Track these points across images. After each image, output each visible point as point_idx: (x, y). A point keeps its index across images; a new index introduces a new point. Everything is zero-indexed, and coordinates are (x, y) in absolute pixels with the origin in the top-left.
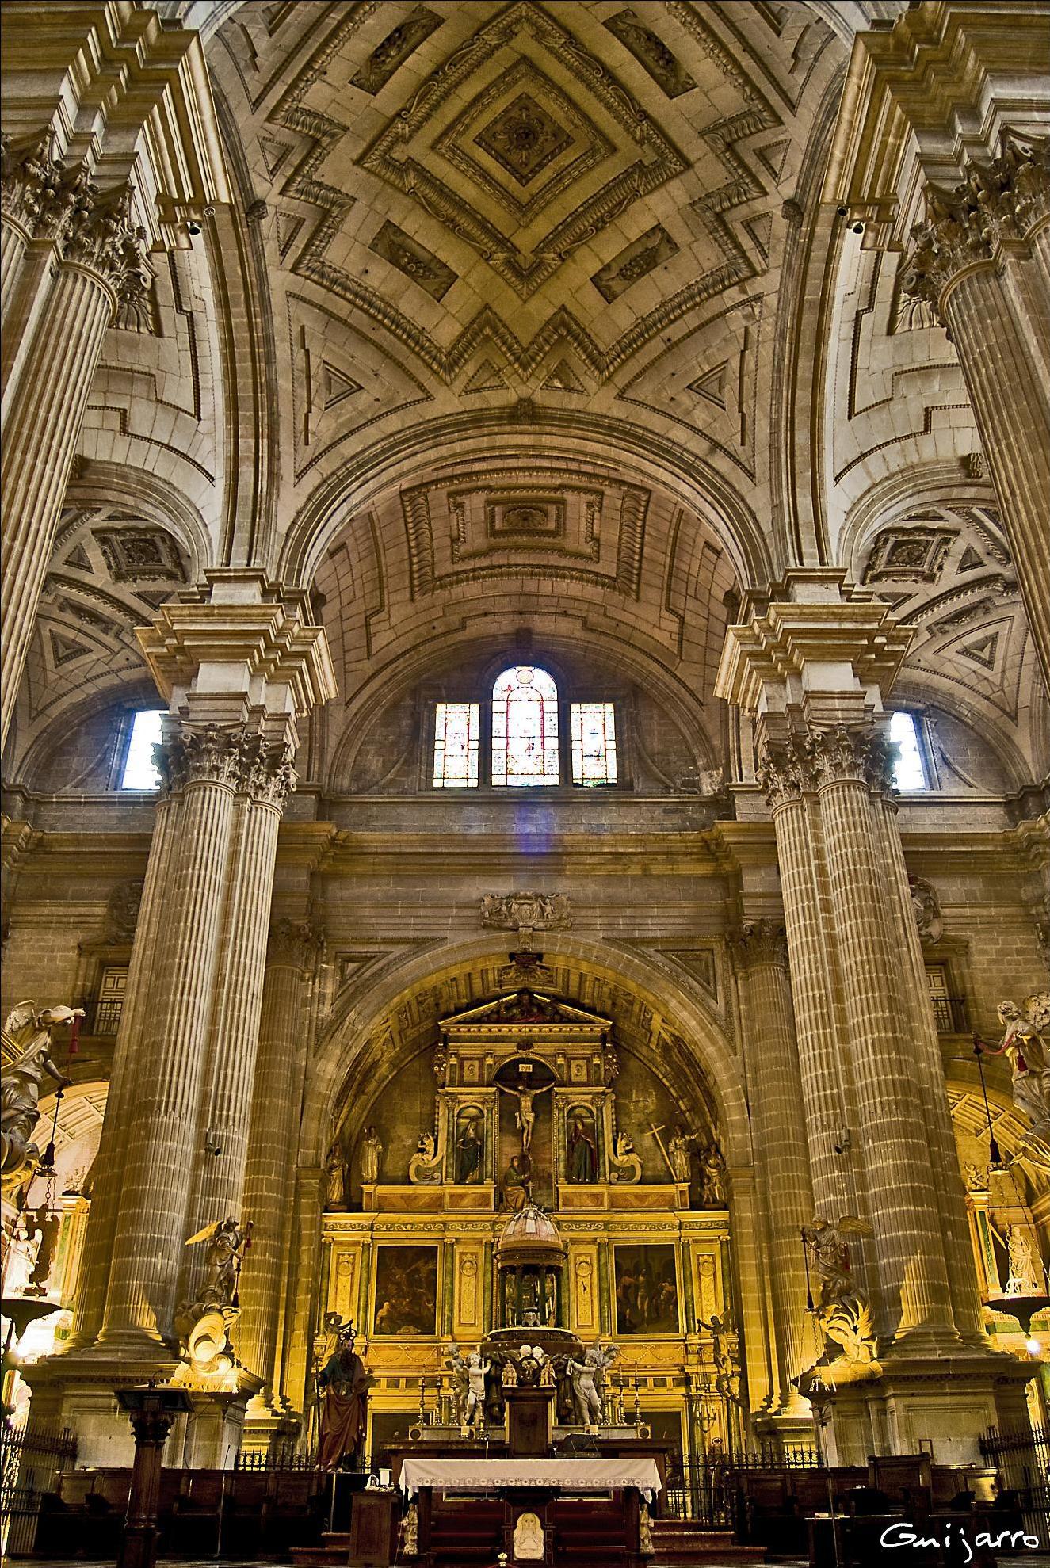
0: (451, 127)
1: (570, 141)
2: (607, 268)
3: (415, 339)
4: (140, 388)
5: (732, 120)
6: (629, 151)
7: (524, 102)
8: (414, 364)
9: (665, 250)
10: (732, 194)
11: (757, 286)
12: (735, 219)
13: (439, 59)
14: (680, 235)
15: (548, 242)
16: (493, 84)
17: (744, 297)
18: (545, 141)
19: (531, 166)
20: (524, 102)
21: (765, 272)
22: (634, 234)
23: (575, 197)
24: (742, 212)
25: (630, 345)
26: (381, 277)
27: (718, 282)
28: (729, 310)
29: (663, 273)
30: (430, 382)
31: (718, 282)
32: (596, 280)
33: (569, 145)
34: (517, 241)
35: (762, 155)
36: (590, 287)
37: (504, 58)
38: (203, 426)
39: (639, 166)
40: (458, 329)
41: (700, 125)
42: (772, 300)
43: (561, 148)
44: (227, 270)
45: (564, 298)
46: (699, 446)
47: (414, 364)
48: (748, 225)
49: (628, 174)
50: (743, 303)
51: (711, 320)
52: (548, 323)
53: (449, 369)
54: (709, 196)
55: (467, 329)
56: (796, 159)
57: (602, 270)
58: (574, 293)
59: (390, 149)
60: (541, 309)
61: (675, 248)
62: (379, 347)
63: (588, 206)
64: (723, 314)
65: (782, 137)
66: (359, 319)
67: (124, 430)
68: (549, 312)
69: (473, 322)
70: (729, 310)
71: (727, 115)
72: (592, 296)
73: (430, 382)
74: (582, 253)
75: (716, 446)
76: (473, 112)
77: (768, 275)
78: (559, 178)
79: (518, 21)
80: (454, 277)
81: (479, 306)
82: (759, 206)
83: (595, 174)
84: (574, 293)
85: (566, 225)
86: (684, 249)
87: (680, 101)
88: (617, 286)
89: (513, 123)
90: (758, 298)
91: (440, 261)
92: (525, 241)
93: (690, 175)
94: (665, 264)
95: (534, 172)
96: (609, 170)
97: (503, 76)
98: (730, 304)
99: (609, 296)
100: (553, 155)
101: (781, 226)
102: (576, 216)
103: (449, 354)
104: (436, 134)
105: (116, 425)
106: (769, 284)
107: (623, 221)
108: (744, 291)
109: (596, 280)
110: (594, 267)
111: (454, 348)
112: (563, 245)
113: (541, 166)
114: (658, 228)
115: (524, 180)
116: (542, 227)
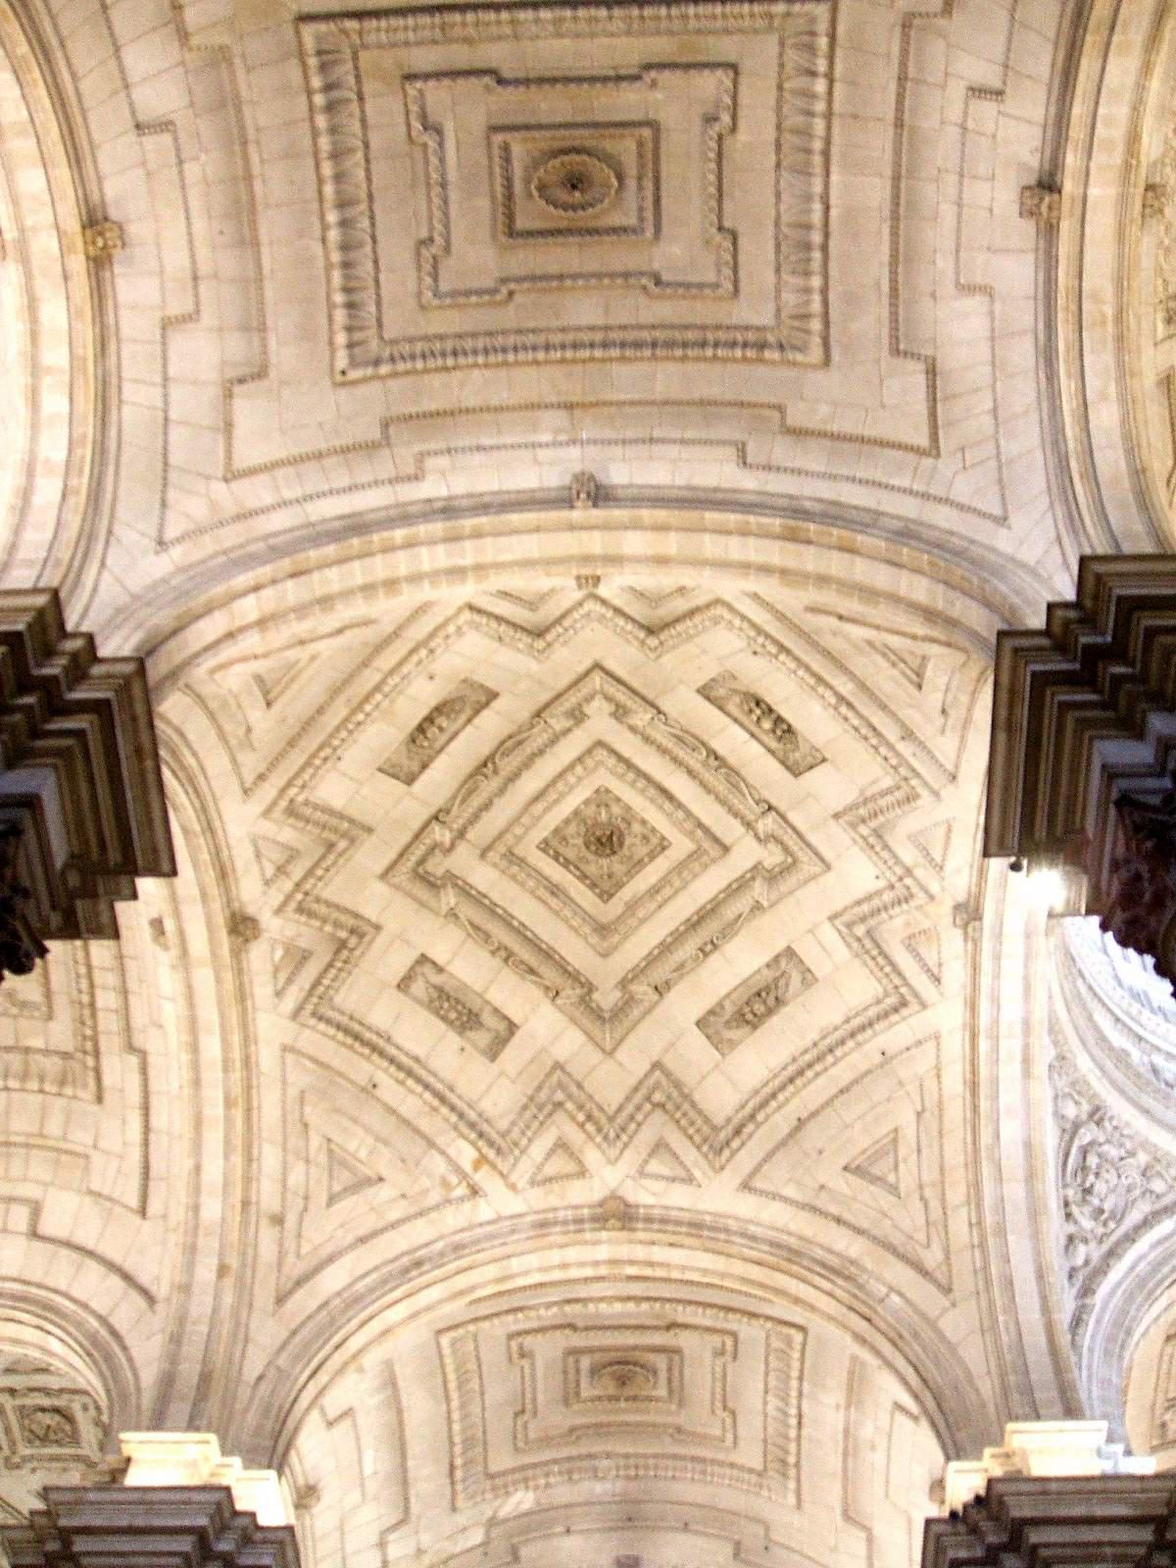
0: (629, 765)
1: (606, 896)
2: (440, 970)
3: (327, 752)
4: (237, 346)
5: (693, 1105)
6: (607, 975)
7: (602, 799)
8: (297, 759)
9: (483, 1038)
10: (591, 1117)
11: (483, 1177)
12: (563, 1126)
13: (732, 760)
14: (513, 1056)
15: (466, 890)
16: (689, 814)
17: (468, 1167)
18: (597, 866)
19: (562, 850)
20: (602, 799)
21: (513, 1187)
22: (496, 996)
23: (526, 909)
24: (575, 1136)
25: (356, 1035)
26: (420, 695)
27: (476, 1128)
28: (443, 1153)
29: (456, 1047)
30: (269, 791)
31: (476, 1128)
32: (423, 959)
33: (600, 896)
34: (462, 848)
35: (660, 1147)
36: (415, 955)
37: (728, 828)
38: (219, 489)
39: (590, 988)
40: (338, 803)
41: (669, 1062)
42: (484, 1211)
43: (593, 886)
44: (503, 540)
45: (391, 926)
46: (268, 1195)
47: (297, 759)
48: (561, 1145)
49: (574, 976)
50: (458, 1170)
51: (417, 1131)
52: (357, 916)
53: (291, 811)
54: (580, 1086)
55: (341, 816)
56: (678, 1198)
57: (434, 964)
58: (402, 938)
59: (608, 698)
60: (374, 900)
61: (493, 1052)
62: (320, 711)
63: (521, 932)
64: (431, 1144)
65: (697, 1174)
66: (370, 678)
67: (167, 325)
68: (370, 912)
69: (351, 821)
70: (443, 1153)
71: (697, 1097)
72: (399, 962)
73: (269, 791)
74: (455, 934)
75: (278, 1220)
76: (652, 791)
77: (510, 1194)
78: (555, 890)
79: (589, 699)
80: (410, 780)
81: (367, 820)
82: (592, 1157)
83: (565, 932)
84: (402, 938)
85: (491, 909)
86: (495, 1067)
87: (697, 1038)
88: (418, 988)
89: (623, 826)
90: (475, 1191)
91: (431, 759)
92: (465, 862)
93: (596, 1056)
94: (468, 1047)
95: (556, 857)
96: (576, 951)
97: (700, 825)
98: (451, 1151)
99: (404, 984)
100: (583, 877)
101: (583, 1194)
102: (506, 920)
103: (306, 803)
104: (618, 746)
105: (175, 309)
106: (499, 1201)
107: (509, 977)
108: (477, 1166)
109: (423, 959)
110: (439, 955)
111: (316, 807)
112: (467, 911)
113: (566, 864)
114: (512, 1027)
115: (545, 846)
116: (484, 877)
